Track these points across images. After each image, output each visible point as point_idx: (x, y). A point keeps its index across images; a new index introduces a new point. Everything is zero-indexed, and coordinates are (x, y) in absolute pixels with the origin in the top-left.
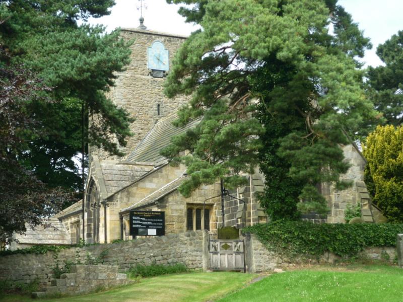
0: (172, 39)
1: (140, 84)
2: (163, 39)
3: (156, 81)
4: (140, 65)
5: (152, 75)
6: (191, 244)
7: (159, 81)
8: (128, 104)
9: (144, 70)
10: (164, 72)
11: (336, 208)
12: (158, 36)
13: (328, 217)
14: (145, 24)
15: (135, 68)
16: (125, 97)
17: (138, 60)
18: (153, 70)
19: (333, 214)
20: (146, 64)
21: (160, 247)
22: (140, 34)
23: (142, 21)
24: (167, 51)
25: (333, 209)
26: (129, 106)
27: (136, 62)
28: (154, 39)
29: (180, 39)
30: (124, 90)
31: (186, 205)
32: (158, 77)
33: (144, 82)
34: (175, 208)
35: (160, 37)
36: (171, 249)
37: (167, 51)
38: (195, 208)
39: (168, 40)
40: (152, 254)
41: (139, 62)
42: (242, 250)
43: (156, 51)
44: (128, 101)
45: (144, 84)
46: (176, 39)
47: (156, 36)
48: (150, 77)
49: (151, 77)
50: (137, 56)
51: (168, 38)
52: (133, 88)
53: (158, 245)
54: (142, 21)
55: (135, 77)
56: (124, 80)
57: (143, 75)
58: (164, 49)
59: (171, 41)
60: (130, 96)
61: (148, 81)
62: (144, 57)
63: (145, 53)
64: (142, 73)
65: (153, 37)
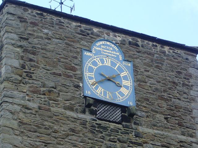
0: (140, 41)
1: (64, 128)
2: (119, 38)
3: (105, 128)
4: (64, 85)
5: (93, 113)
7: (112, 127)
9: (73, 98)
10: (124, 108)
12: (106, 31)
15: (50, 91)
17: (60, 75)
18: (98, 102)
20: (78, 87)
22: (62, 19)
27: (52, 77)
28: (98, 36)
30: (20, 138)
32: (110, 121)
33: (72, 126)
35: (111, 34)
39: (130, 43)
41: (61, 80)
43: (102, 61)
45: (73, 130)
46: (151, 43)
47: (101, 30)
48: (88, 117)
49: (93, 117)
51: (130, 39)
52: (45, 138)
55: (49, 110)
56: (21, 115)
57: (71, 109)
58: (121, 58)
59: (138, 45)
61: (84, 123)
63: (76, 61)
64: (68, 104)
65: (95, 30)
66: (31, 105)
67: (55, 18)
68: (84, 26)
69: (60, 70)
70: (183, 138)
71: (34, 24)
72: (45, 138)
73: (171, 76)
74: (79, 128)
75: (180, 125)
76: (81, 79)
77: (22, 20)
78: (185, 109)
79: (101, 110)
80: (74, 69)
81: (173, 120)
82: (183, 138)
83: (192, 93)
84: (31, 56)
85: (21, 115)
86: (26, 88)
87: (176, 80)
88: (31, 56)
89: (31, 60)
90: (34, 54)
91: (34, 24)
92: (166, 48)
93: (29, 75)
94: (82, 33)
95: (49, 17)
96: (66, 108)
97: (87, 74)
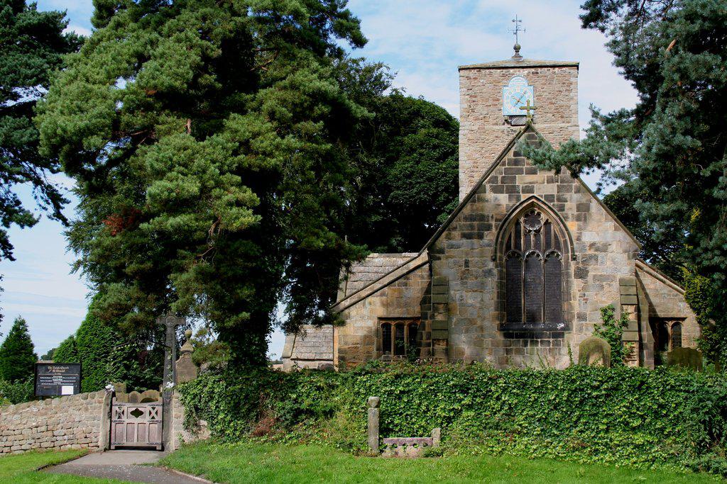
0: (539, 70)
1: (491, 138)
2: (526, 71)
3: (515, 131)
5: (508, 123)
6: (87, 409)
8: (474, 167)
11: (579, 321)
13: (566, 335)
14: (521, 53)
16: (469, 157)
18: (511, 117)
19: (574, 329)
21: (46, 414)
22: (492, 71)
23: (517, 49)
24: (532, 87)
25: (575, 323)
26: (476, 169)
28: (513, 74)
29: (551, 69)
30: (468, 148)
31: (376, 321)
34: (359, 325)
35: (521, 70)
36: (60, 416)
37: (532, 87)
38: (407, 322)
40: (34, 424)
41: (491, 108)
42: (158, 418)
44: (474, 162)
46: (546, 69)
48: (507, 126)
49: (509, 126)
50: (487, 100)
51: (533, 70)
52: (481, 145)
53: (43, 411)
54: (517, 49)
56: (469, 136)
58: (527, 85)
59: (537, 73)
60: (477, 156)
62: (498, 100)
63: (499, 95)
65: (512, 71)
66: (474, 128)
67: (487, 71)
68: (504, 70)
69: (490, 102)
70: (563, 125)
71: (475, 79)
72: (481, 145)
73: (557, 87)
74: (500, 134)
75: (562, 117)
76: (502, 105)
77: (468, 78)
78: (567, 106)
79: (514, 121)
80: (498, 100)
81: (557, 115)
82: (563, 125)
83: (571, 94)
84: (474, 99)
85: (469, 136)
86: (471, 118)
87: (561, 89)
88: (474, 99)
89: (474, 101)
90: (476, 97)
91: (475, 79)
92: (556, 69)
93: (473, 111)
94: (503, 75)
95: (483, 71)
96: (493, 125)
97: (505, 101)
